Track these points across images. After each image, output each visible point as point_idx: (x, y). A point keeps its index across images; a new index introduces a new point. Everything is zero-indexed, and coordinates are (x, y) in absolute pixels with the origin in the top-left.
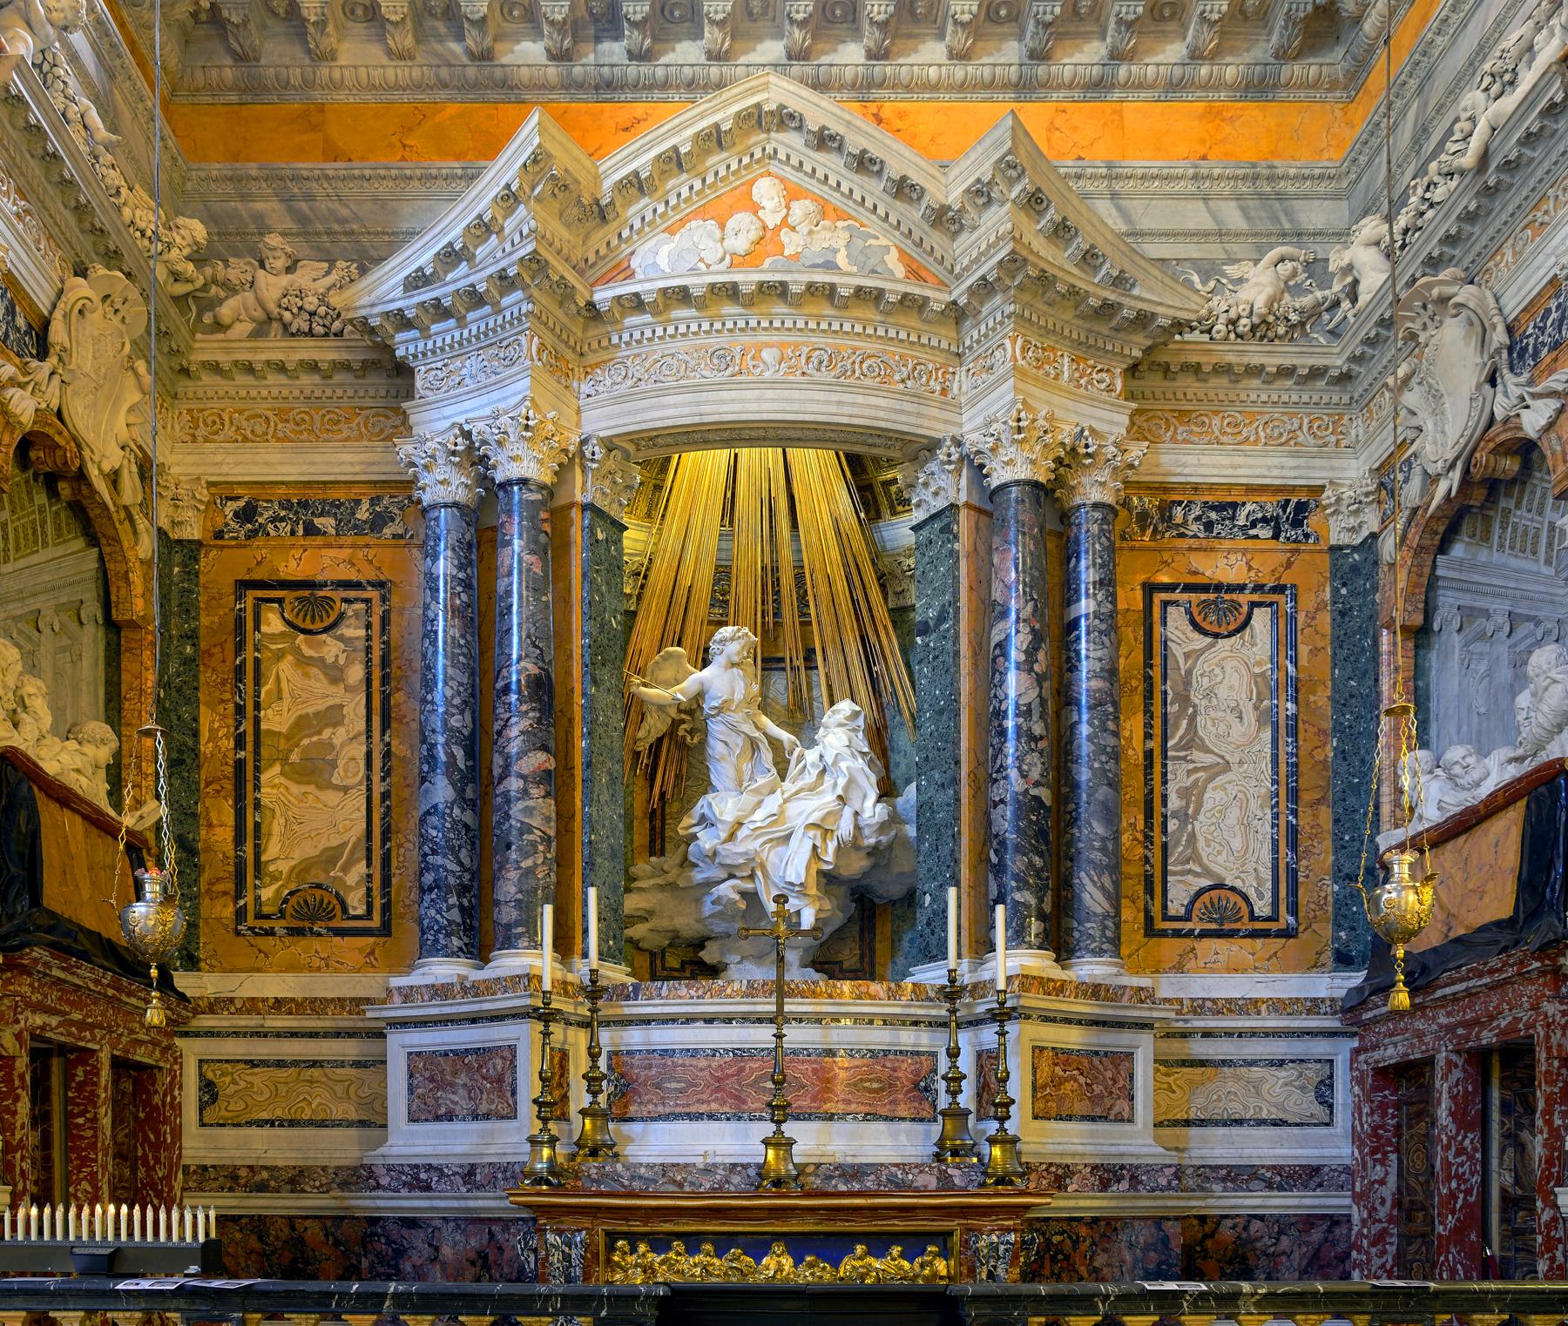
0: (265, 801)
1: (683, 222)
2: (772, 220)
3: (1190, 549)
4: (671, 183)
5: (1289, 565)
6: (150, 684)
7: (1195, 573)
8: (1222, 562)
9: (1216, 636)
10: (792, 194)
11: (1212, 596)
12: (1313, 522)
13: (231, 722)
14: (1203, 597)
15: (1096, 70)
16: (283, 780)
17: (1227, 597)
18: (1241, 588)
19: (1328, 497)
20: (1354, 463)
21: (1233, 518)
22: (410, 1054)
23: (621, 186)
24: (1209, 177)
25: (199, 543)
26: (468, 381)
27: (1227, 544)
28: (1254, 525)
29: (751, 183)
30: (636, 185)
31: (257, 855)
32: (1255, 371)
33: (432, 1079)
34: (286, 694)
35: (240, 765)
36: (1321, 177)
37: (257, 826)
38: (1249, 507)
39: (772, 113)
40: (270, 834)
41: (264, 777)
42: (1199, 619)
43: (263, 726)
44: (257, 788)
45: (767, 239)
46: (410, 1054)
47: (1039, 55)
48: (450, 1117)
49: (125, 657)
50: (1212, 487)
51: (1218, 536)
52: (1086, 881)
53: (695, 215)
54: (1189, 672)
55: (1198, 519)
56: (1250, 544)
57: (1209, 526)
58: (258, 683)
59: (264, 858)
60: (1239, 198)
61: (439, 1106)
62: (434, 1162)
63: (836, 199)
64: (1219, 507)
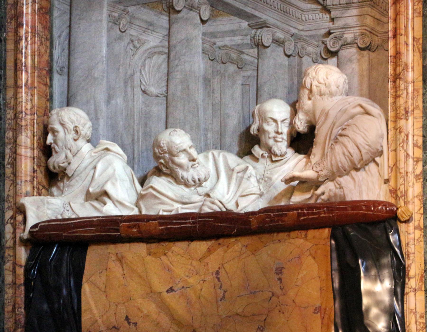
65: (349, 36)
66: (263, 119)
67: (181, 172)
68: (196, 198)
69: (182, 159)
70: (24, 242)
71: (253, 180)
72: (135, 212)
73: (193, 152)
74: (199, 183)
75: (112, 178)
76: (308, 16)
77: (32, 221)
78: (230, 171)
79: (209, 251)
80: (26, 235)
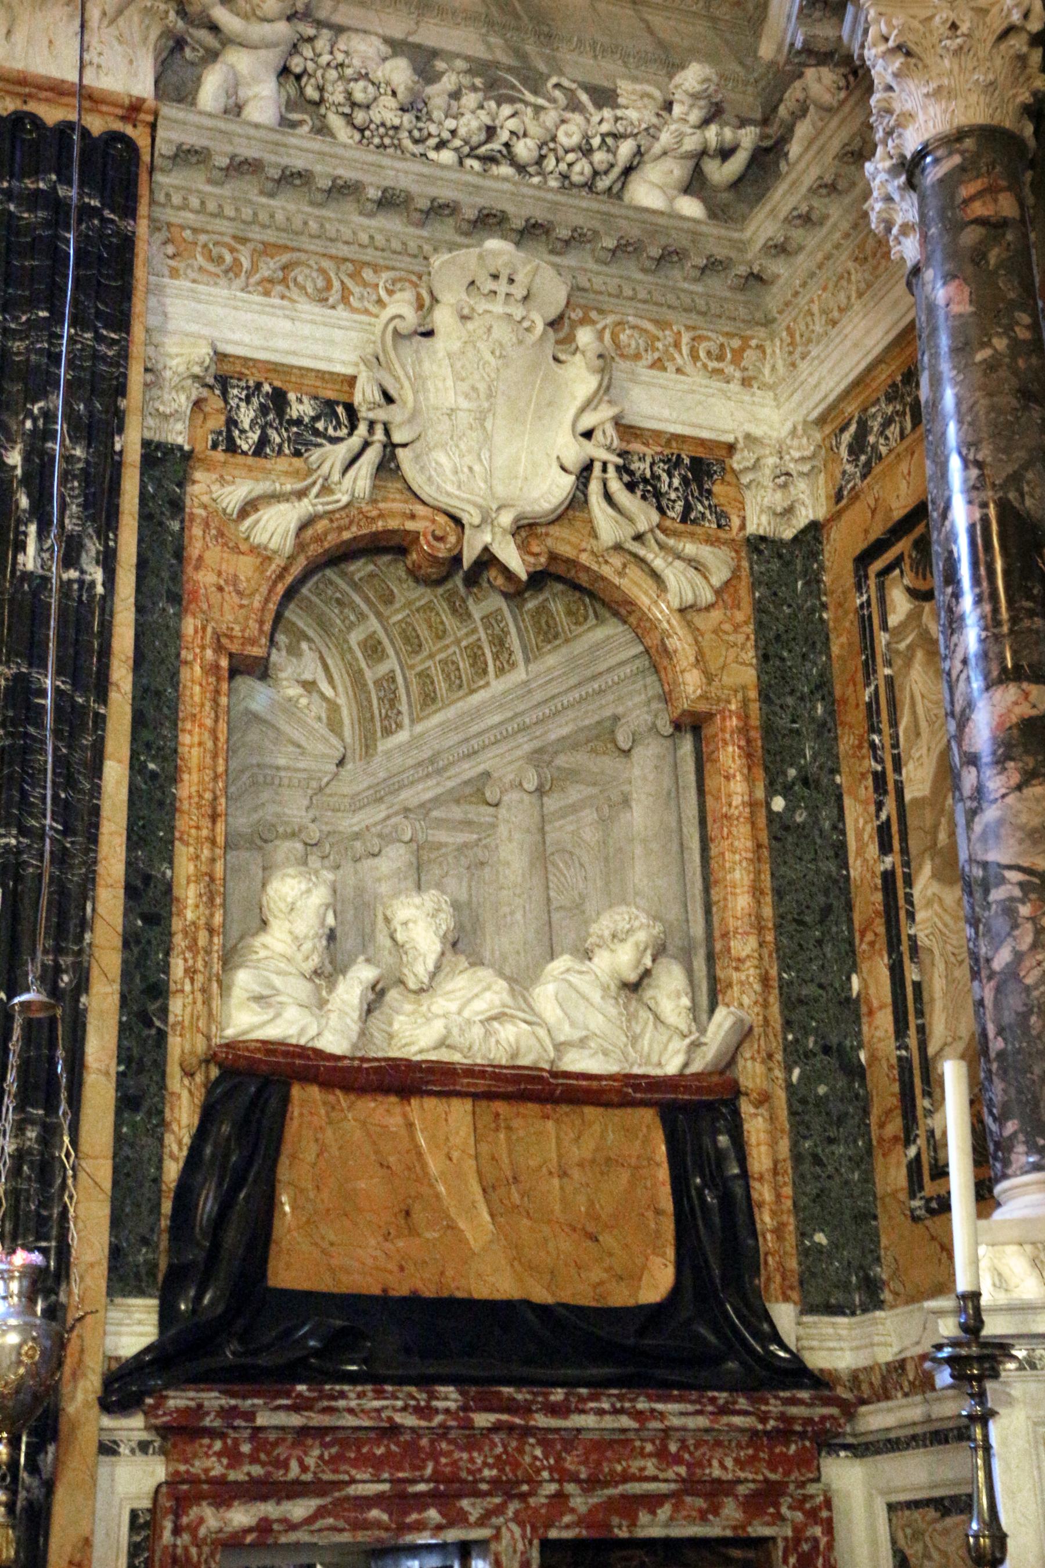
0: (923, 940)
6: (737, 800)
13: (872, 808)
16: (935, 888)
25: (814, 528)
31: (923, 1046)
34: (923, 724)
35: (888, 877)
37: (917, 986)
40: (932, 1000)
41: (917, 892)
43: (908, 797)
44: (911, 916)
49: (708, 766)
58: (894, 724)
59: (931, 1050)
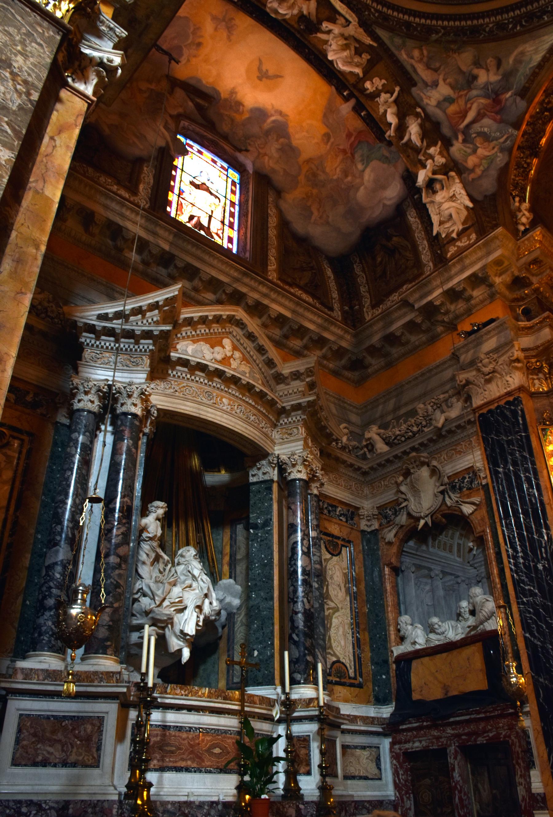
1: (198, 341)
2: (229, 354)
3: (325, 519)
4: (199, 326)
5: (350, 533)
7: (326, 528)
8: (333, 527)
9: (333, 555)
10: (235, 348)
11: (331, 539)
12: (356, 519)
14: (329, 538)
15: (299, 348)
17: (335, 540)
18: (338, 538)
19: (361, 512)
20: (366, 503)
21: (335, 511)
22: (21, 715)
23: (185, 319)
24: (329, 394)
26: (112, 364)
27: (334, 520)
28: (341, 515)
29: (223, 338)
30: (189, 322)
32: (344, 462)
33: (35, 735)
36: (354, 407)
38: (339, 509)
39: (237, 320)
42: (328, 546)
45: (225, 360)
46: (21, 715)
47: (286, 337)
48: (45, 764)
50: (330, 498)
51: (332, 517)
52: (319, 654)
53: (203, 340)
54: (326, 567)
55: (326, 508)
56: (340, 522)
57: (329, 512)
60: (335, 404)
61: (37, 755)
62: (35, 798)
63: (247, 356)
64: (332, 506)
65: (483, 575)
66: (460, 608)
67: (437, 631)
68: (443, 638)
69: (436, 626)
70: (394, 662)
71: (460, 629)
72: (425, 646)
73: (440, 623)
74: (443, 633)
75: (417, 637)
76: (471, 571)
77: (395, 654)
78: (452, 627)
79: (447, 656)
80: (393, 659)
